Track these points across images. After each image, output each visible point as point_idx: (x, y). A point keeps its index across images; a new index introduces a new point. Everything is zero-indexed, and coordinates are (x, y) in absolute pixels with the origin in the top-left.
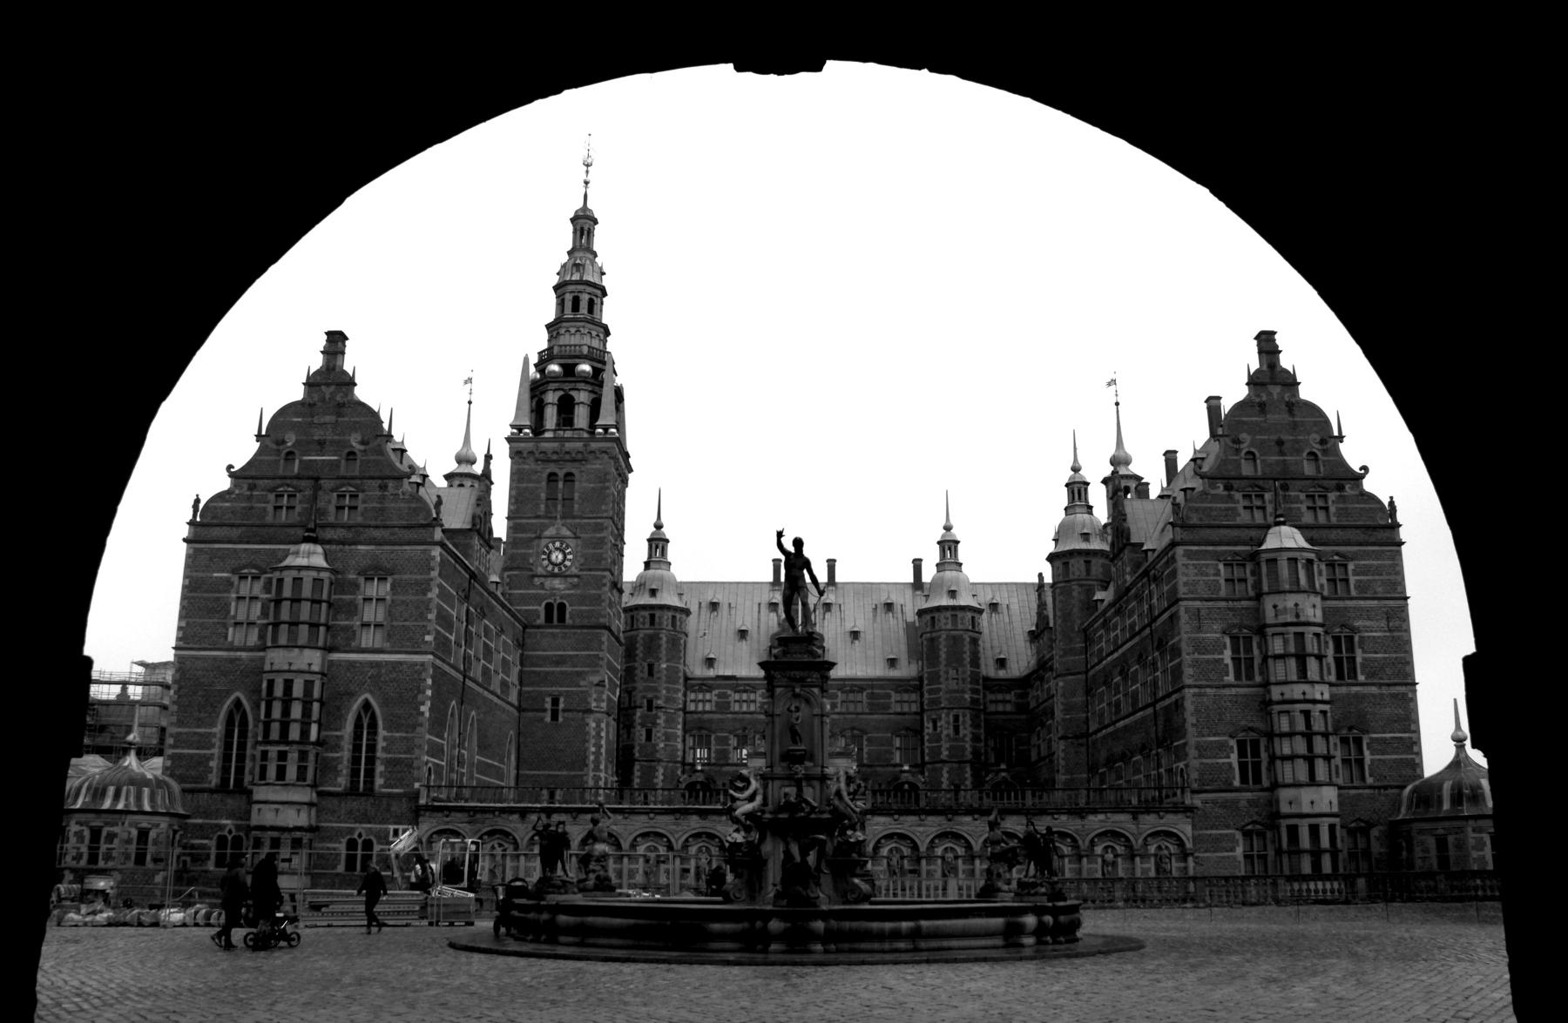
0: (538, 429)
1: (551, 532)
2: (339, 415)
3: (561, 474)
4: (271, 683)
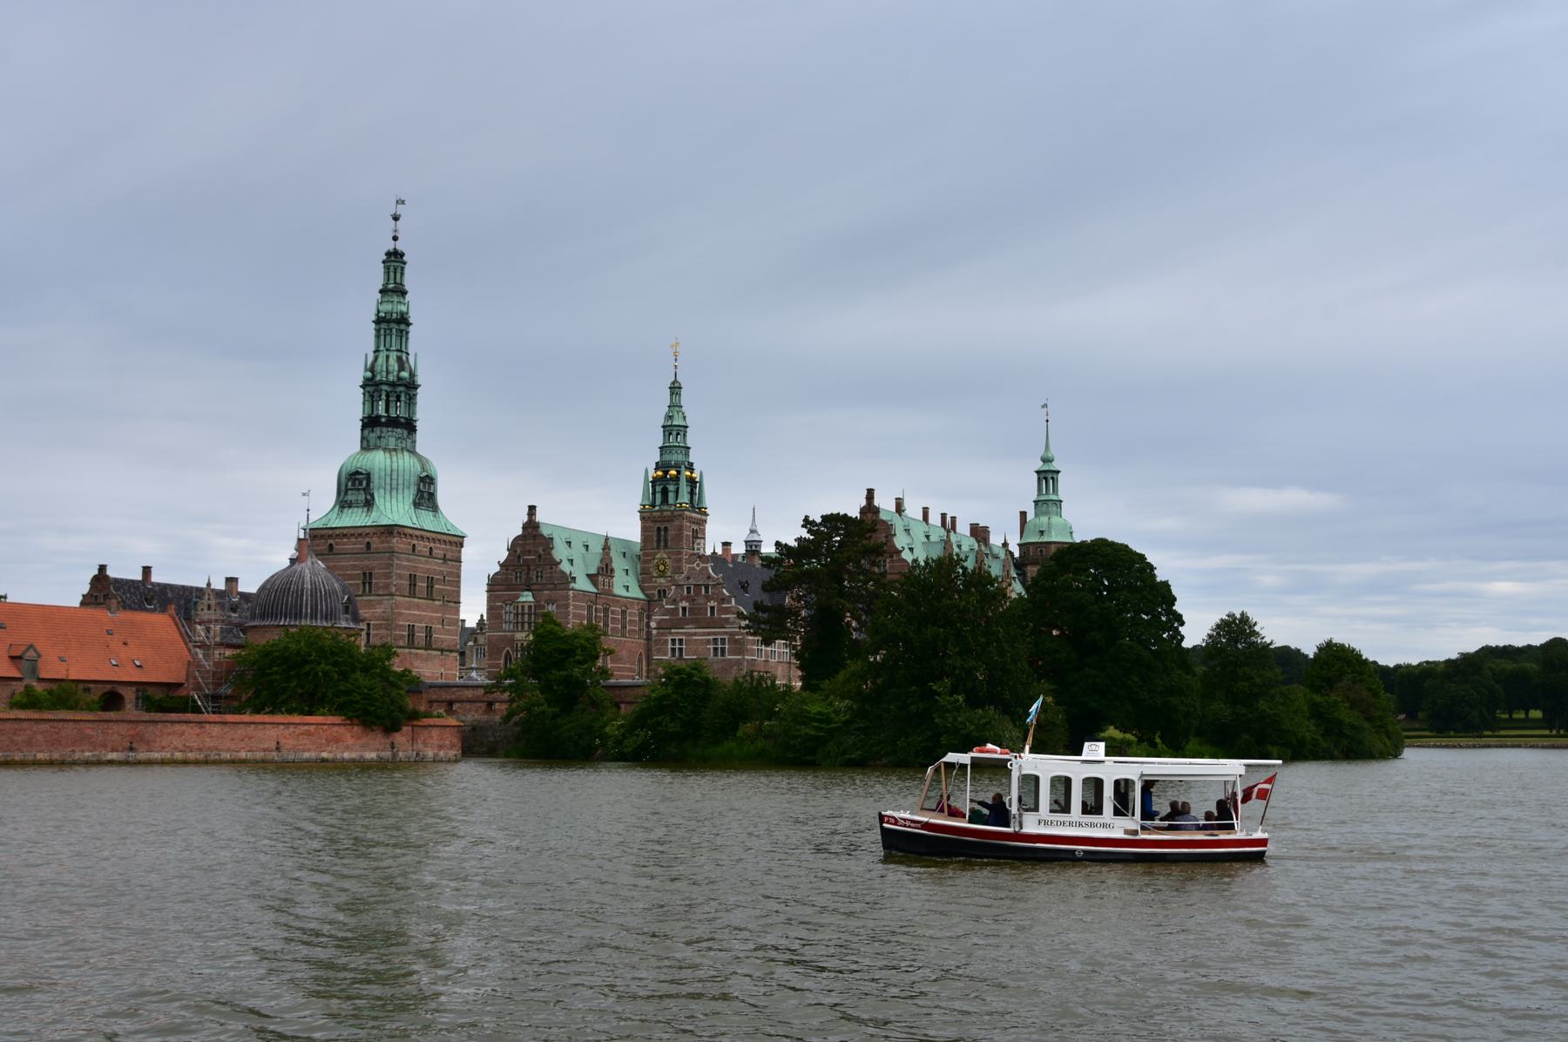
0: (653, 505)
1: (658, 556)
2: (534, 539)
3: (662, 527)
4: (517, 644)
